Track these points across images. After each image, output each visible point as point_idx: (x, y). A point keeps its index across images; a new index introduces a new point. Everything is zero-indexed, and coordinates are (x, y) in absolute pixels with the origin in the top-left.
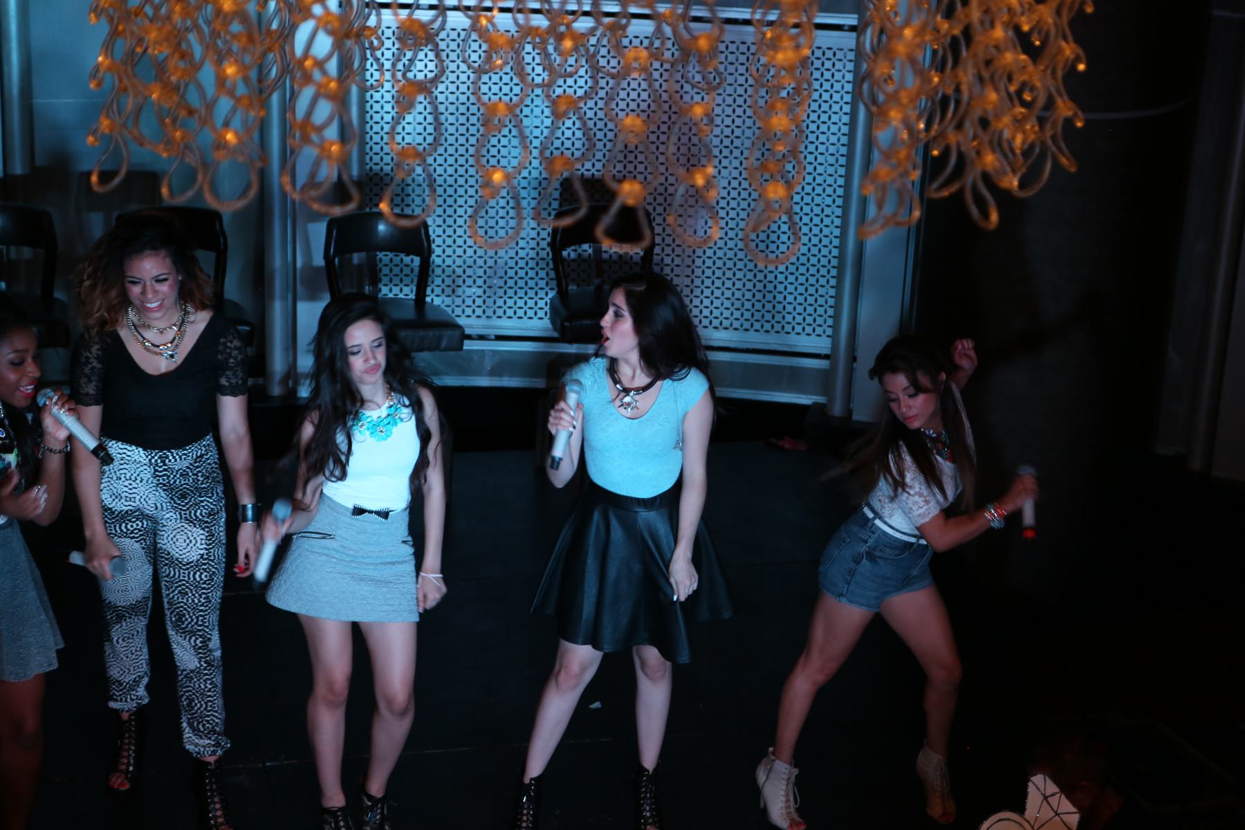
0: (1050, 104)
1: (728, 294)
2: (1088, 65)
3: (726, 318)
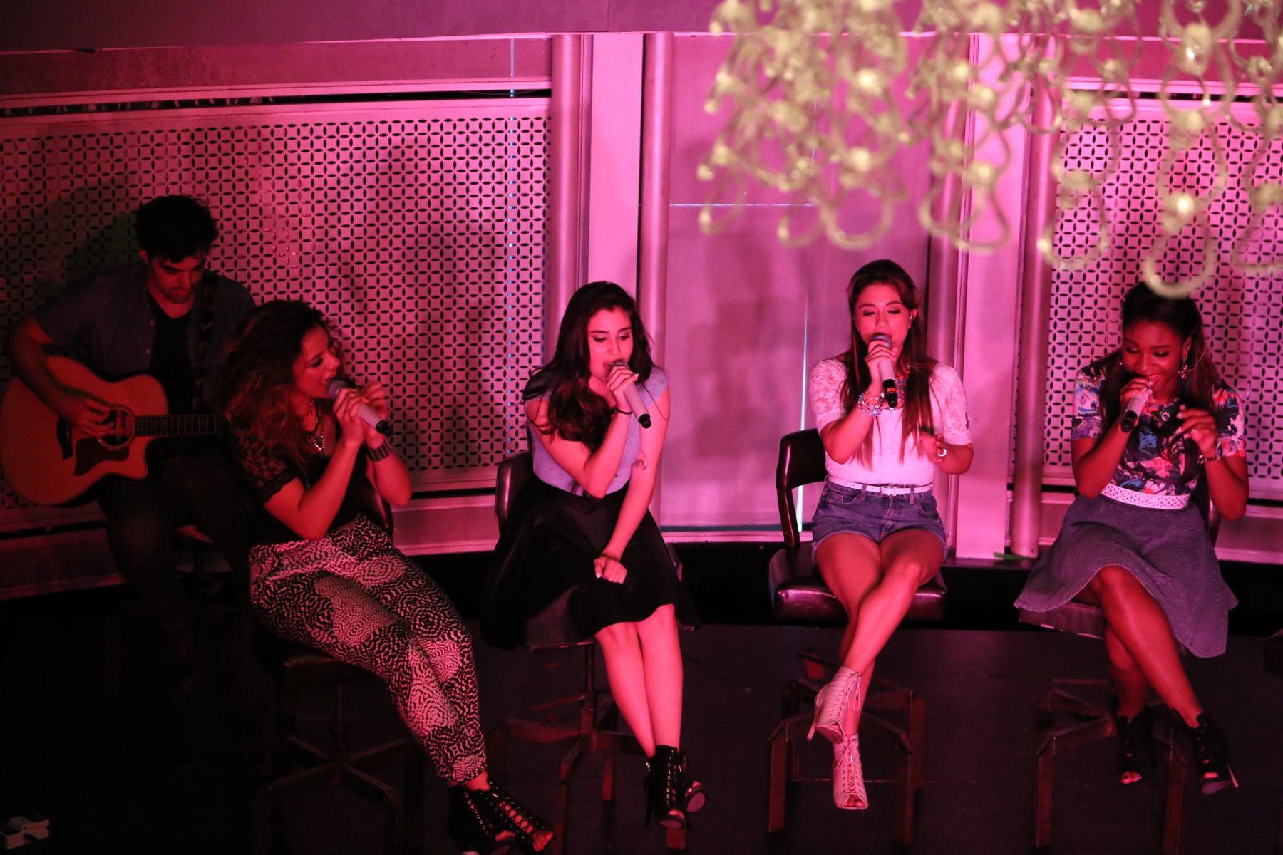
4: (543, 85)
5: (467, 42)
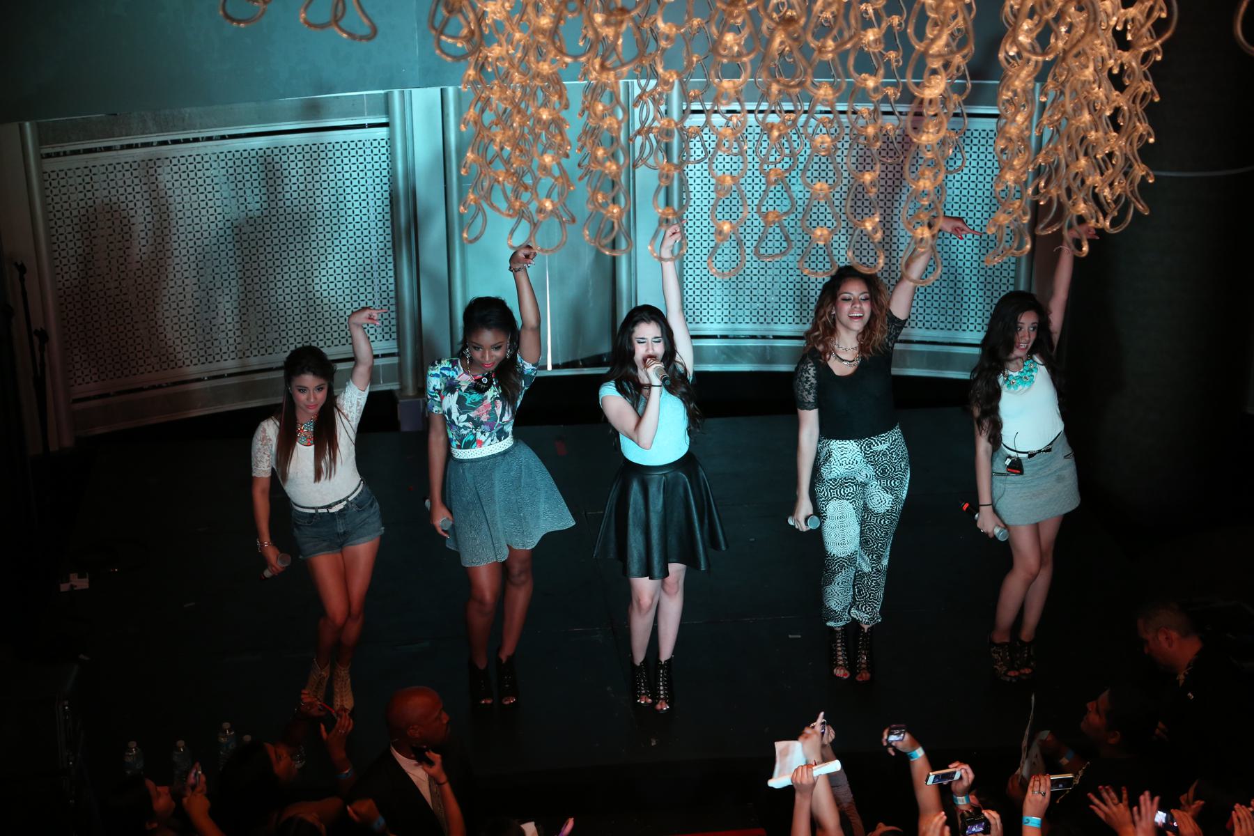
0: (1131, 166)
1: (936, 304)
2: (1156, 139)
3: (935, 322)
4: (384, 120)
5: (337, 97)
